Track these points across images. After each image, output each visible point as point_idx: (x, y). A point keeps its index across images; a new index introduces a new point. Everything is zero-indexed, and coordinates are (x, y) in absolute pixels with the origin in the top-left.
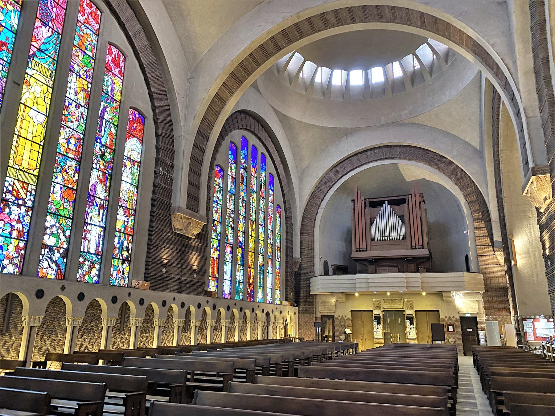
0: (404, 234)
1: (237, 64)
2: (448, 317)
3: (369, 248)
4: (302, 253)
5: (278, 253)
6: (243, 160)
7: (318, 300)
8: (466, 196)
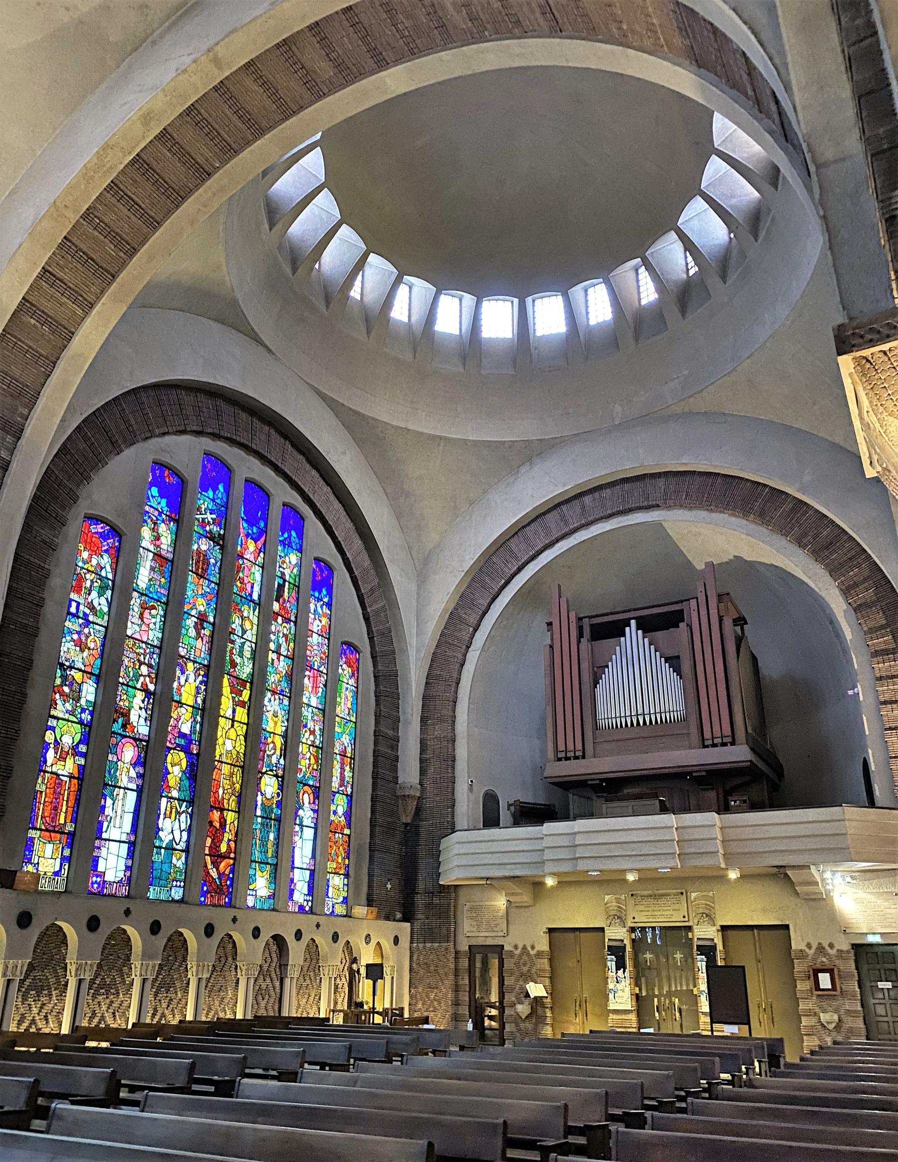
0: (681, 707)
1: (74, 218)
2: (815, 946)
3: (589, 751)
4: (423, 772)
5: (339, 773)
6: (210, 517)
7: (462, 900)
8: (846, 591)
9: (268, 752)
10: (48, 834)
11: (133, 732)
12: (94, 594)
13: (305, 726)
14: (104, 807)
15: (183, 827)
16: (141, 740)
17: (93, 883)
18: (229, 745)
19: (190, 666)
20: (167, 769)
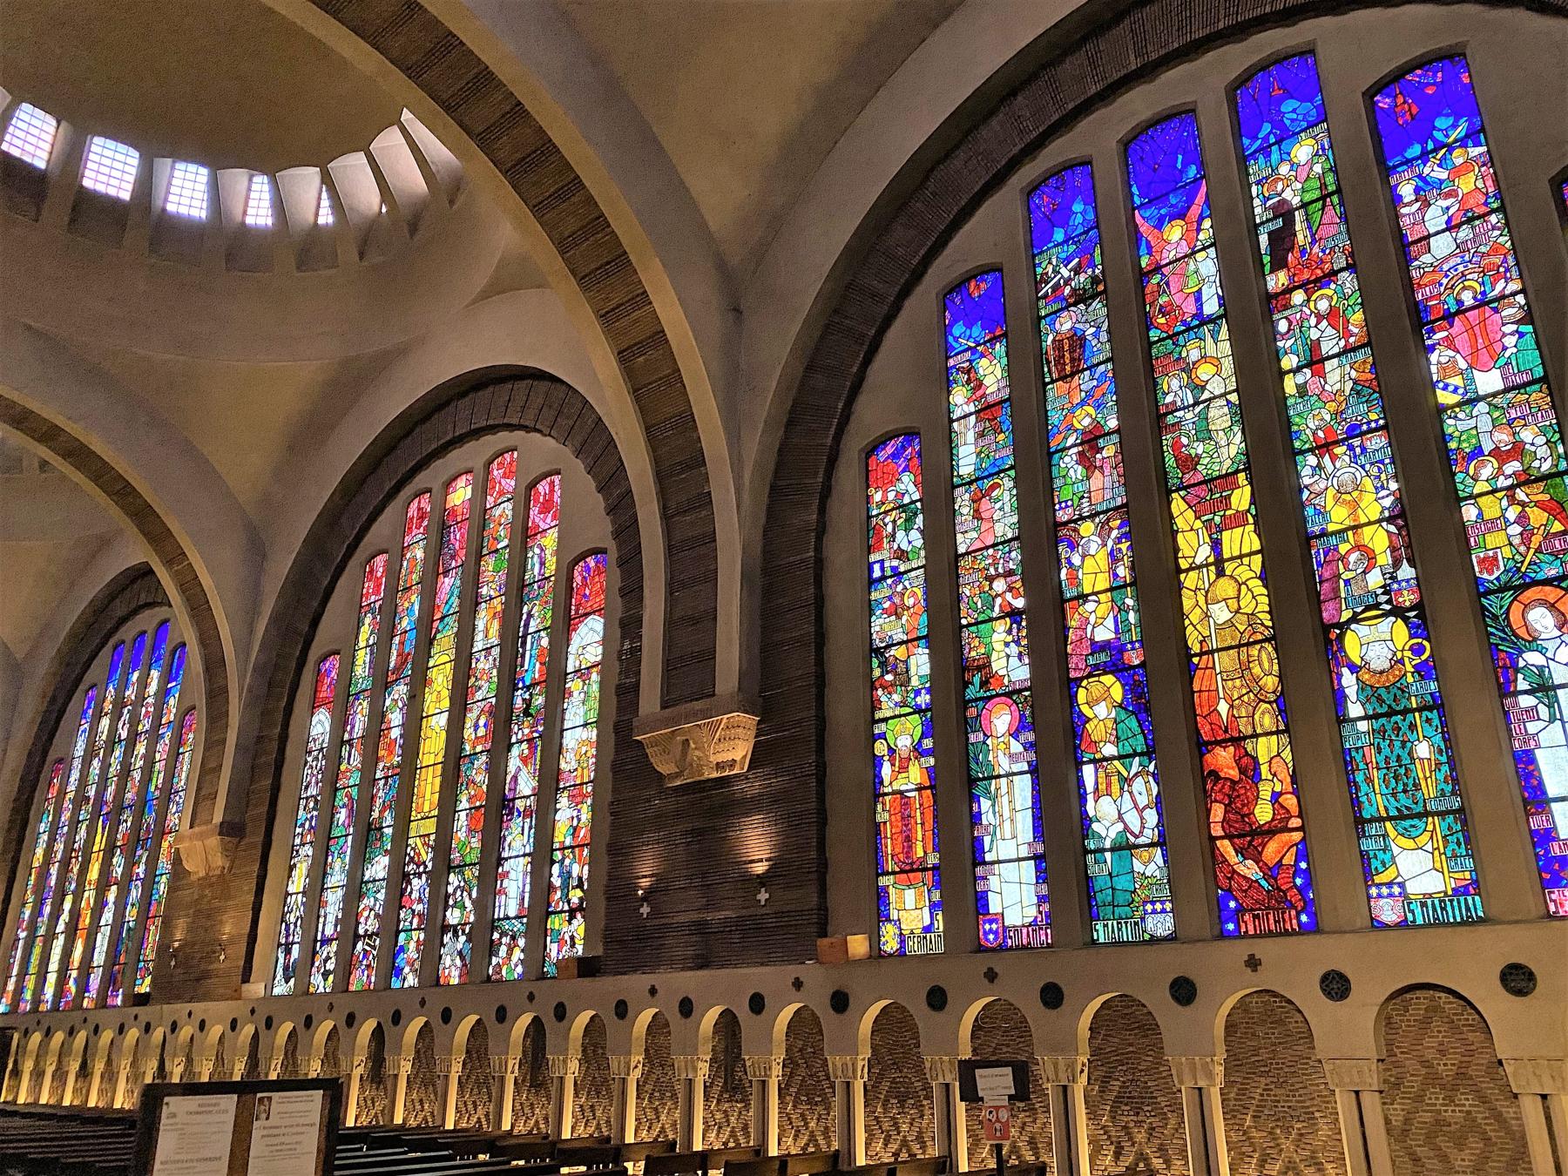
9: (1347, 575)
10: (904, 876)
11: (1002, 684)
12: (900, 534)
13: (1478, 452)
14: (980, 814)
15: (1142, 801)
16: (1019, 691)
17: (986, 933)
18: (1221, 614)
19: (1087, 528)
20: (1081, 714)
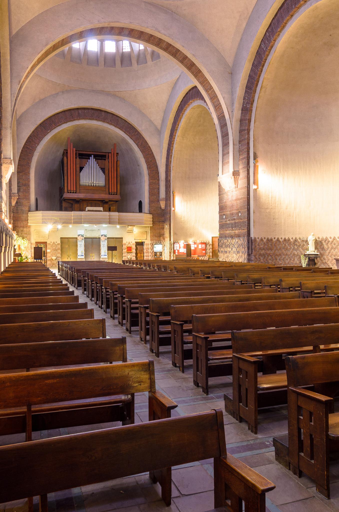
0: (104, 183)
3: (78, 191)
